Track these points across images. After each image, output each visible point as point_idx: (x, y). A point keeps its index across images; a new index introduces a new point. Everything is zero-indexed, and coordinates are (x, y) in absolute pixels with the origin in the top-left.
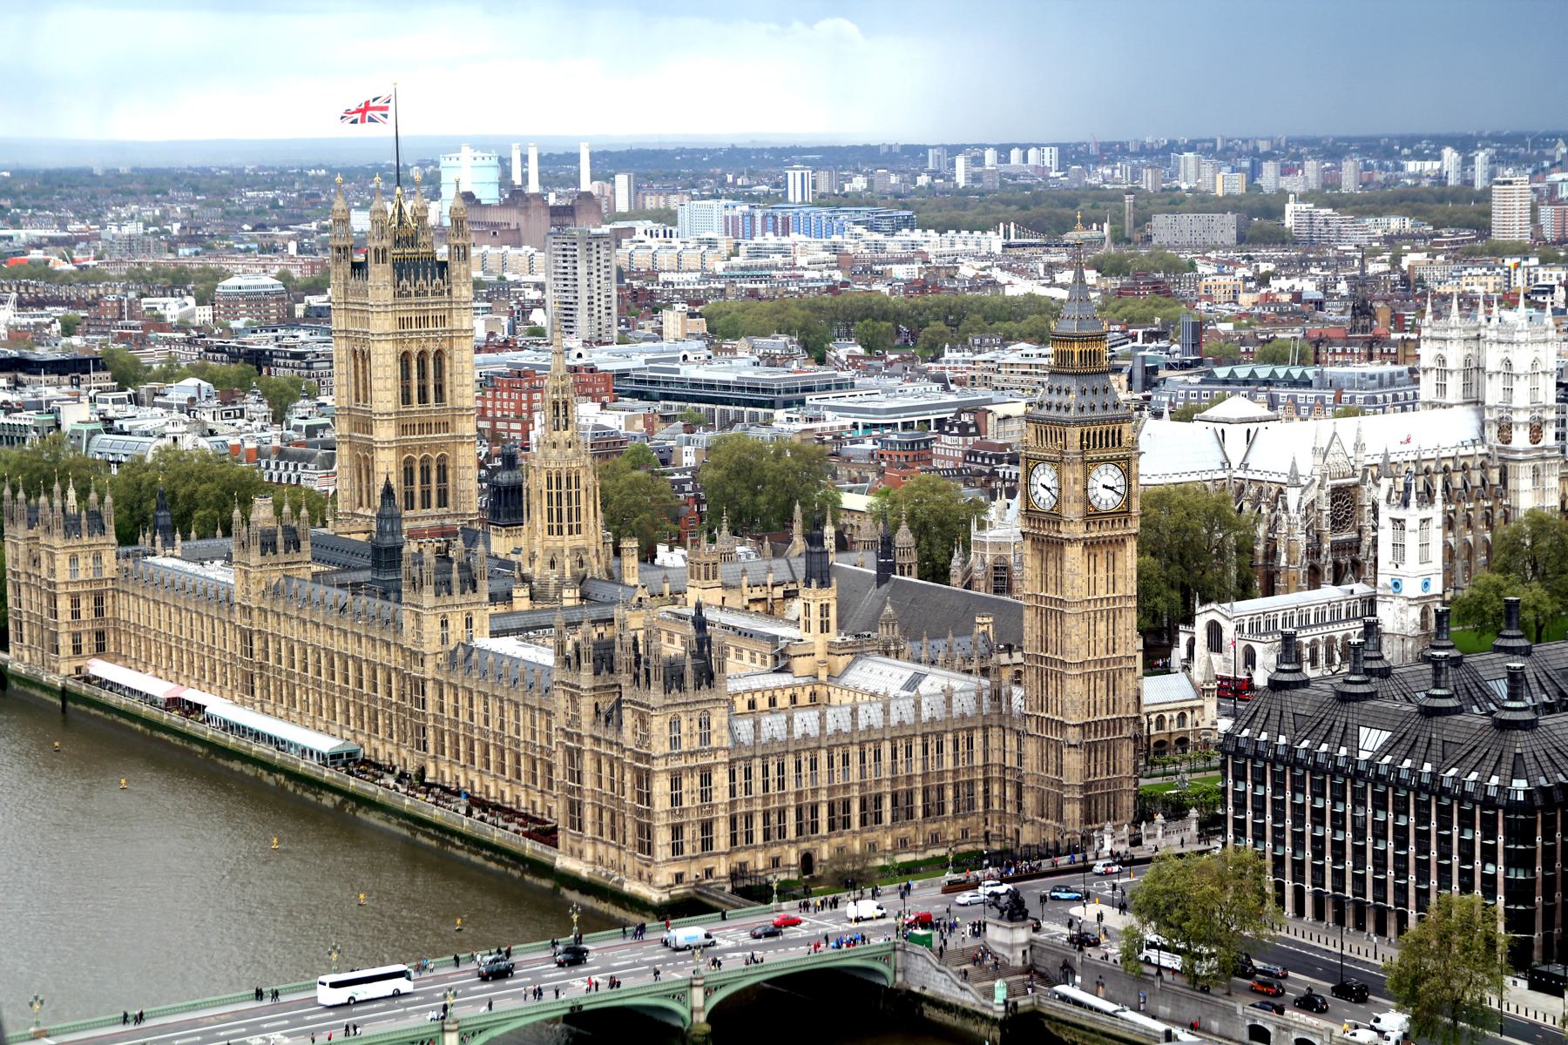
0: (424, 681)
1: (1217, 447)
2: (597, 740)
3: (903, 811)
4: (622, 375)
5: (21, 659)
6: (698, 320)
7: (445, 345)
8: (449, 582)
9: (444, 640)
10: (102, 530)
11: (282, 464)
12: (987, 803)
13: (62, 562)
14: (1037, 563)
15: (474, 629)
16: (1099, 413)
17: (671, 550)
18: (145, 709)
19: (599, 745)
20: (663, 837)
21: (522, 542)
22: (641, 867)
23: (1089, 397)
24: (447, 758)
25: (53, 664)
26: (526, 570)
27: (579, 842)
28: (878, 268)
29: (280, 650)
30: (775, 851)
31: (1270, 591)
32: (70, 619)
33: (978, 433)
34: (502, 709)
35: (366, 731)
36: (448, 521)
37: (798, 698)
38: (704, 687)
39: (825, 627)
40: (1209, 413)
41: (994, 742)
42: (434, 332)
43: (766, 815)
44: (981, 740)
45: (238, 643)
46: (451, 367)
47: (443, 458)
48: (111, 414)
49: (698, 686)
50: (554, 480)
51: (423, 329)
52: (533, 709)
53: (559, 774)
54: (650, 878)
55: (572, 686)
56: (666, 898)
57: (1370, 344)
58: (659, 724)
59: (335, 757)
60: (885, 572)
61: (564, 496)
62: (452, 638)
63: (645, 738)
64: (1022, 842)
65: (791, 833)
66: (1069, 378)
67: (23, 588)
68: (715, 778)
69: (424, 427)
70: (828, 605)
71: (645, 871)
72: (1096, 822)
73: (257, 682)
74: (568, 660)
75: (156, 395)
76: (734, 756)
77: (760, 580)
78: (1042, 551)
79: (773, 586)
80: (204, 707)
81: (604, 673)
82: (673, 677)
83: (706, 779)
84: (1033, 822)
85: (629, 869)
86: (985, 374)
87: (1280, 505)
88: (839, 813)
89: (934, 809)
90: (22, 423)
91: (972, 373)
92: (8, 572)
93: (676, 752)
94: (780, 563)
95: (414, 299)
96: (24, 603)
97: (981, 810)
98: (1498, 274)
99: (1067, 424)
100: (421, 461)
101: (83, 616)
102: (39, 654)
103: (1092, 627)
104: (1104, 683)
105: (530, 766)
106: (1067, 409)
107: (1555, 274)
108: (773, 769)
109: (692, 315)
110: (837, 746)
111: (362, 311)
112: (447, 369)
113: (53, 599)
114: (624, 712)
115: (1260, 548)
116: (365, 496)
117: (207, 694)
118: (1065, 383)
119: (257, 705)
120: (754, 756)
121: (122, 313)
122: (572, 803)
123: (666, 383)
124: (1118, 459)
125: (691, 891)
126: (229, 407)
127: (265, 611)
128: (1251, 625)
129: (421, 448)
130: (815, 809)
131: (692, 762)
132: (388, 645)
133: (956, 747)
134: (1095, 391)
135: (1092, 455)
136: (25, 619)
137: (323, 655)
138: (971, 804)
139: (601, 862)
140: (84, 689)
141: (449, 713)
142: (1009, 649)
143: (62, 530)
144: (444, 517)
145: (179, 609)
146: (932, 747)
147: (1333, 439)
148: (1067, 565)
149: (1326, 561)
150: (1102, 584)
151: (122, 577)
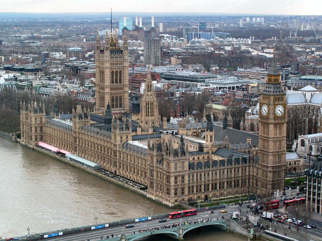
0: (116, 151)
1: (304, 98)
2: (157, 167)
4: (162, 74)
7: (122, 70)
9: (121, 141)
10: (42, 112)
11: (83, 96)
13: (33, 120)
14: (262, 128)
15: (128, 139)
16: (278, 93)
17: (174, 118)
18: (52, 154)
19: (158, 169)
20: (173, 191)
21: (139, 117)
23: (276, 89)
24: (122, 169)
25: (31, 143)
26: (140, 124)
27: (153, 191)
28: (222, 47)
29: (83, 142)
30: (199, 195)
31: (316, 132)
33: (246, 90)
35: (103, 162)
36: (122, 111)
37: (205, 157)
38: (183, 156)
39: (211, 141)
40: (302, 89)
41: (251, 170)
42: (119, 67)
44: (248, 169)
45: (73, 139)
46: (123, 75)
47: (121, 96)
48: (44, 83)
49: (182, 156)
50: (147, 104)
51: (117, 66)
52: (142, 159)
54: (169, 200)
55: (152, 155)
56: (173, 205)
58: (172, 165)
60: (225, 126)
61: (150, 107)
62: (123, 141)
64: (257, 193)
65: (203, 190)
66: (271, 85)
67: (24, 125)
68: (185, 177)
70: (212, 136)
71: (168, 199)
74: (151, 149)
75: (54, 77)
76: (190, 172)
77: (195, 128)
78: (264, 125)
80: (65, 154)
81: (159, 152)
82: (176, 153)
83: (183, 177)
86: (248, 75)
87: (319, 112)
88: (214, 186)
89: (236, 185)
90: (24, 84)
93: (176, 171)
94: (200, 124)
95: (115, 59)
96: (24, 128)
97: (248, 186)
100: (116, 97)
101: (38, 132)
102: (28, 140)
103: (275, 144)
104: (278, 157)
105: (141, 172)
106: (271, 92)
108: (199, 175)
109: (178, 59)
111: (102, 61)
112: (122, 75)
113: (31, 128)
115: (314, 121)
116: (102, 105)
117: (66, 151)
118: (270, 86)
122: (151, 182)
124: (282, 104)
125: (179, 204)
126: (71, 81)
128: (311, 140)
129: (116, 94)
130: (208, 185)
131: (180, 174)
132: (108, 142)
133: (242, 171)
134: (277, 88)
135: (276, 103)
137: (93, 143)
140: (38, 148)
142: (255, 146)
143: (33, 112)
144: (120, 110)
146: (236, 171)
148: (270, 129)
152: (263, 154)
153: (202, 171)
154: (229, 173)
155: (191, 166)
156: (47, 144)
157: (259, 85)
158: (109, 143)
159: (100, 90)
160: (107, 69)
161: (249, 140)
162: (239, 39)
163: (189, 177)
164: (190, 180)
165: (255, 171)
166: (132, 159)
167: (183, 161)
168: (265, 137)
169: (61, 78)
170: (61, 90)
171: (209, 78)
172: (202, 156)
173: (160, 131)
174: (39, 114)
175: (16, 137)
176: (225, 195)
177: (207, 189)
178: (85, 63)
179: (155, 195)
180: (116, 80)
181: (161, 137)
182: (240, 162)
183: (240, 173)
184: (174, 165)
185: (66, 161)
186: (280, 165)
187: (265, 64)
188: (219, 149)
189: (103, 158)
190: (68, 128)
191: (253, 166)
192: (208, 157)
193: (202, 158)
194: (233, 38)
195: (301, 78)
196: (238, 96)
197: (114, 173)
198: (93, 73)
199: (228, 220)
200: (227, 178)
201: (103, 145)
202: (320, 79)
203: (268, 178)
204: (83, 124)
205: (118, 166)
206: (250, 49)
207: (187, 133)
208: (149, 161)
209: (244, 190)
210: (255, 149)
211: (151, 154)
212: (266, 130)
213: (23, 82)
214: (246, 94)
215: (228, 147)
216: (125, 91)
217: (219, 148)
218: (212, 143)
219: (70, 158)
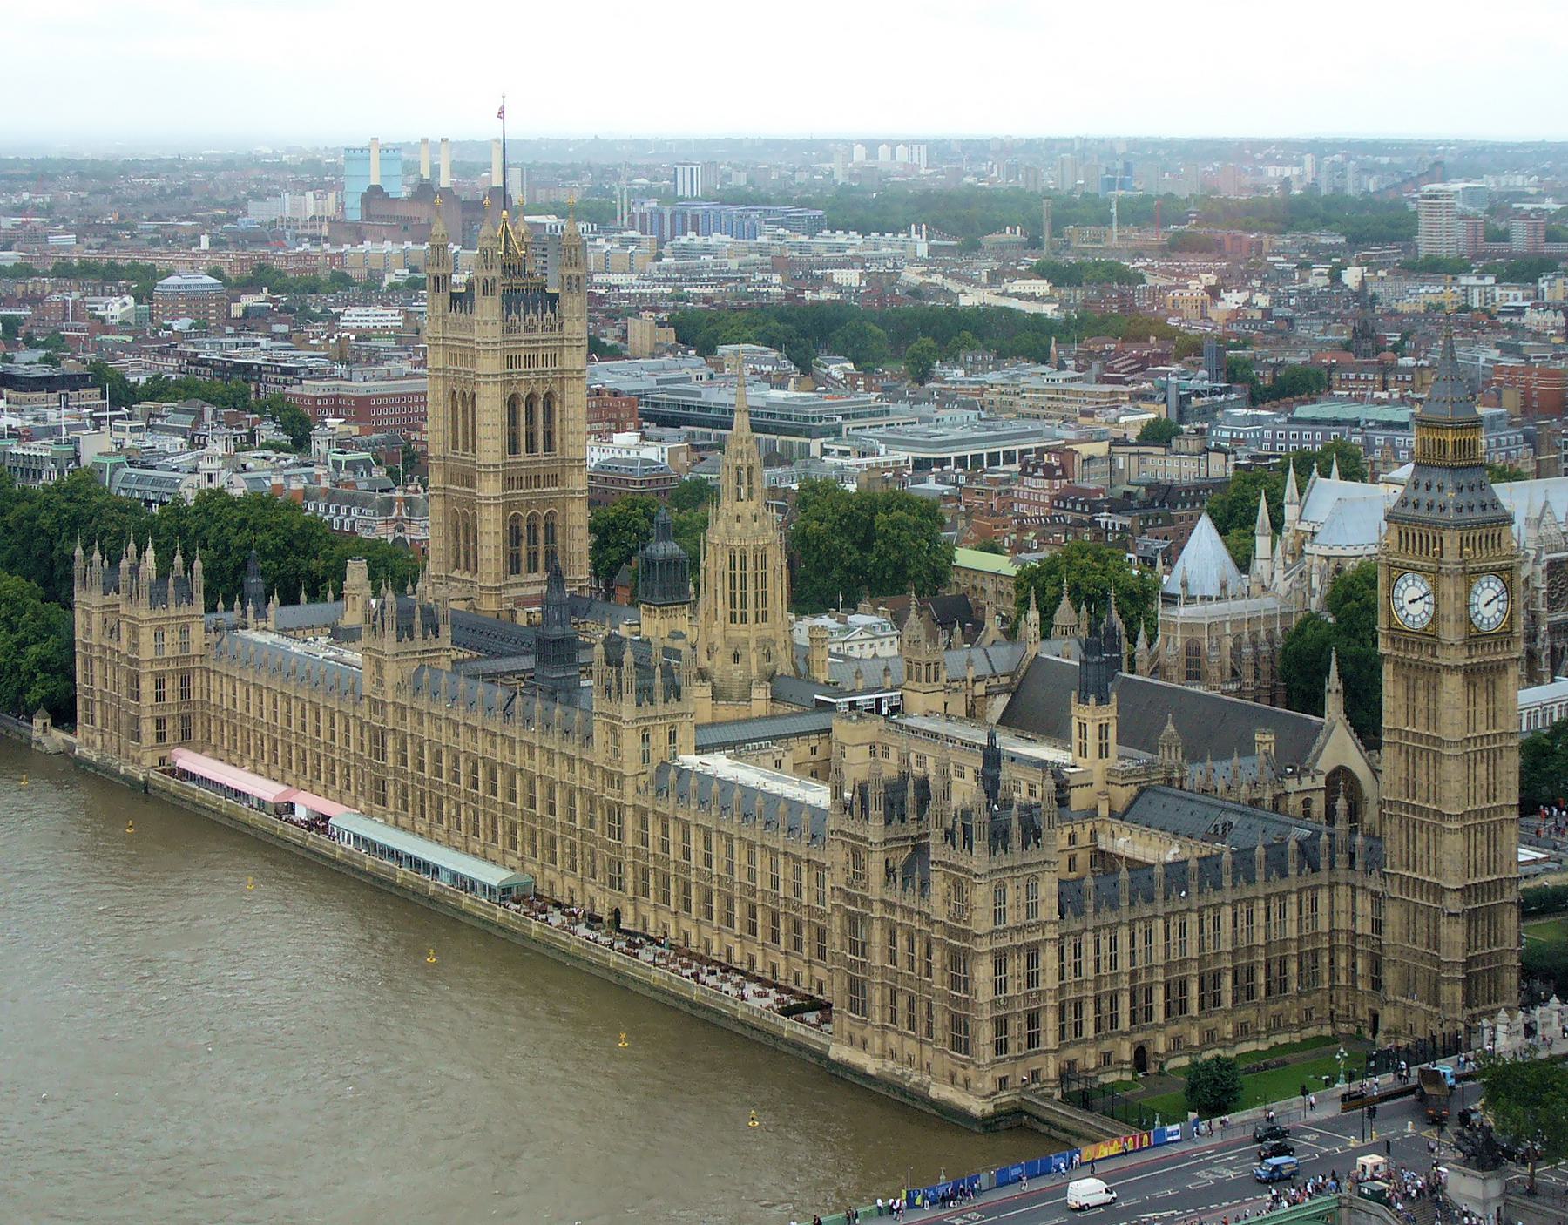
2: (889, 906)
5: (92, 745)
6: (666, 329)
7: (556, 387)
8: (650, 689)
9: (646, 758)
13: (146, 637)
15: (678, 744)
19: (894, 913)
21: (682, 623)
25: (132, 753)
26: (704, 662)
27: (863, 1029)
28: (819, 272)
30: (1106, 1045)
32: (154, 703)
33: (1065, 476)
34: (729, 850)
37: (1078, 837)
39: (1103, 751)
42: (544, 373)
44: (1327, 901)
45: (366, 743)
48: (128, 443)
50: (736, 559)
51: (532, 369)
53: (836, 942)
54: (967, 1084)
55: (855, 837)
57: (1386, 369)
58: (981, 896)
59: (506, 891)
63: (962, 908)
65: (1124, 1023)
67: (97, 664)
68: (1042, 957)
71: (960, 1073)
73: (391, 791)
74: (847, 807)
75: (151, 415)
77: (961, 675)
81: (896, 821)
82: (999, 838)
84: (1395, 1003)
88: (1175, 995)
89: (1275, 986)
91: (991, 398)
92: (78, 644)
93: (1001, 927)
94: (977, 654)
96: (97, 680)
97: (1327, 986)
98: (1455, 292)
100: (528, 519)
108: (1105, 944)
109: (661, 324)
113: (135, 679)
117: (322, 799)
119: (389, 817)
121: (66, 314)
127: (403, 708)
129: (529, 504)
132: (571, 759)
136: (98, 699)
138: (1316, 977)
139: (893, 1055)
140: (173, 784)
141: (653, 847)
143: (148, 600)
146: (1275, 910)
149: (1543, 644)
151: (212, 654)
152: (1409, 828)
154: (1239, 922)
155: (1069, 901)
156: (214, 757)
157: (1114, 449)
158: (577, 765)
159: (452, 487)
160: (487, 383)
161: (1265, 741)
162: (874, 235)
163: (1062, 959)
164: (1067, 970)
165: (1364, 908)
166: (714, 854)
172: (1068, 831)
174: (172, 611)
175: (48, 721)
176: (1225, 1039)
178: (255, 344)
180: (531, 437)
181: (829, 730)
182: (1290, 865)
184: (991, 896)
186: (1495, 877)
187: (1053, 348)
191: (1348, 884)
194: (846, 233)
195: (1297, 415)
196: (1028, 502)
198: (327, 393)
199: (1345, 1202)
200: (1234, 953)
202: (1380, 418)
203: (1443, 948)
205: (630, 885)
206: (936, 279)
208: (838, 870)
209: (1308, 1012)
210: (1300, 784)
213: (32, 444)
216: (573, 492)
217: (1142, 791)
219: (455, 876)
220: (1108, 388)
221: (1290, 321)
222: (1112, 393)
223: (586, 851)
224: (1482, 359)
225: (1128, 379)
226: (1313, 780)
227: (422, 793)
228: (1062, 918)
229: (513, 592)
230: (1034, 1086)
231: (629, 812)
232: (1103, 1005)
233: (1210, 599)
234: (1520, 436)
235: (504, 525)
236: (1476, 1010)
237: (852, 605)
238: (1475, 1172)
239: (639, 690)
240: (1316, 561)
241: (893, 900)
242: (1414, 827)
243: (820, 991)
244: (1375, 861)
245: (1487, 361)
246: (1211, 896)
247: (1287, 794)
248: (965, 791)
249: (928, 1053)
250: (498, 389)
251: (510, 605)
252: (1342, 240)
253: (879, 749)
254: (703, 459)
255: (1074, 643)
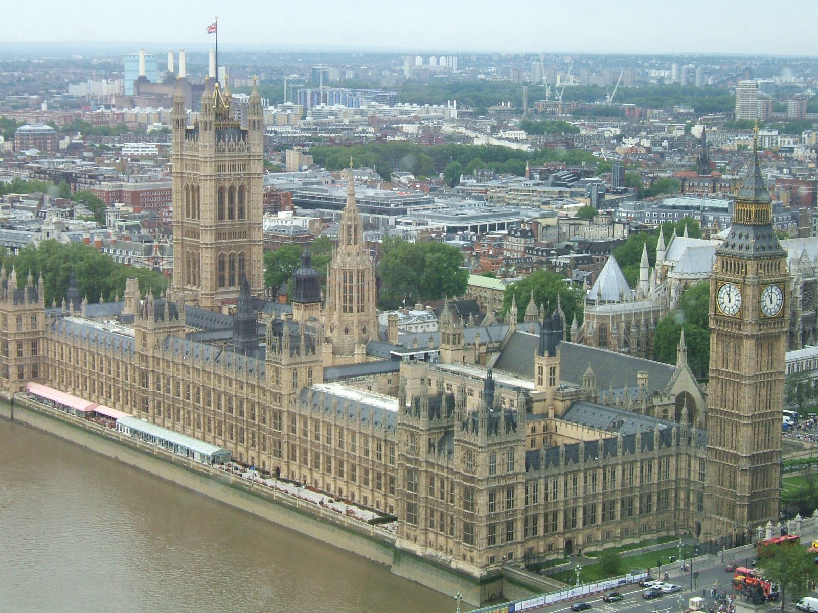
2: (431, 465)
3: (628, 511)
7: (245, 183)
9: (295, 385)
12: (677, 504)
15: (313, 378)
16: (767, 252)
18: (75, 418)
21: (316, 313)
22: (465, 552)
25: (4, 384)
27: (415, 531)
28: (395, 126)
29: (168, 384)
33: (532, 236)
34: (341, 434)
35: (234, 441)
39: (552, 382)
42: (239, 175)
43: (546, 516)
45: (137, 378)
47: (242, 254)
49: (507, 432)
50: (347, 276)
53: (400, 484)
54: (472, 560)
55: (412, 427)
56: (485, 573)
58: (482, 458)
64: (702, 531)
69: (232, 234)
70: (554, 368)
71: (469, 554)
72: (755, 519)
73: (151, 404)
76: (528, 478)
77: (472, 342)
78: (723, 341)
79: (480, 345)
83: (510, 490)
85: (454, 552)
89: (645, 509)
91: (492, 194)
93: (493, 475)
94: (482, 331)
95: (227, 154)
97: (673, 509)
99: (749, 258)
101: (25, 355)
103: (758, 393)
105: (363, 472)
106: (748, 248)
107: (787, 140)
108: (551, 485)
109: (305, 153)
110: (590, 469)
112: (246, 197)
114: (455, 447)
117: (112, 410)
119: (150, 418)
120: (540, 478)
122: (409, 504)
123: (320, 198)
127: (158, 359)
129: (230, 248)
131: (503, 483)
134: (764, 237)
137: (202, 389)
138: (667, 504)
139: (431, 545)
142: (656, 394)
145: (92, 354)
146: (646, 468)
147: (803, 253)
148: (744, 352)
149: (799, 327)
150: (764, 364)
153: (560, 474)
155: (532, 460)
156: (52, 387)
158: (256, 389)
159: (186, 238)
160: (206, 180)
162: (427, 105)
163: (526, 492)
165: (695, 467)
166: (333, 437)
167: (512, 447)
168: (729, 374)
169: (37, 202)
170: (54, 235)
171: (415, 203)
172: (531, 425)
173: (392, 352)
174: (27, 306)
177: (570, 524)
179: (423, 543)
180: (231, 211)
181: (398, 371)
183: (655, 473)
184: (488, 459)
185: (122, 437)
186: (768, 450)
187: (527, 168)
188: (579, 406)
189: (234, 430)
190: (122, 346)
191: (686, 454)
192: (545, 428)
193: (530, 431)
194: (411, 104)
195: (664, 203)
197: (272, 472)
198: (115, 189)
200: (623, 491)
201: (214, 389)
202: (711, 205)
203: (738, 489)
204: (166, 335)
206: (462, 130)
207: (464, 357)
208: (402, 445)
210: (661, 401)
211: (409, 426)
212: (731, 355)
214: (530, 246)
215: (595, 398)
217: (573, 404)
218: (554, 388)
220: (558, 189)
221: (662, 155)
222: (560, 192)
223: (261, 436)
224: (769, 176)
225: (569, 184)
226: (669, 399)
227: (169, 406)
228: (527, 471)
229: (220, 297)
230: (509, 562)
231: (285, 414)
232: (549, 518)
233: (614, 302)
234: (790, 216)
235: (216, 260)
236: (755, 522)
237: (411, 305)
238: (751, 606)
239: (292, 349)
240: (674, 281)
241: (433, 461)
242: (725, 422)
243: (391, 511)
244: (701, 442)
245: (772, 176)
246: (611, 459)
247: (654, 406)
248: (474, 402)
249: (451, 544)
250: (213, 183)
251: (219, 304)
252: (692, 111)
253: (426, 381)
254: (328, 227)
255: (537, 325)
